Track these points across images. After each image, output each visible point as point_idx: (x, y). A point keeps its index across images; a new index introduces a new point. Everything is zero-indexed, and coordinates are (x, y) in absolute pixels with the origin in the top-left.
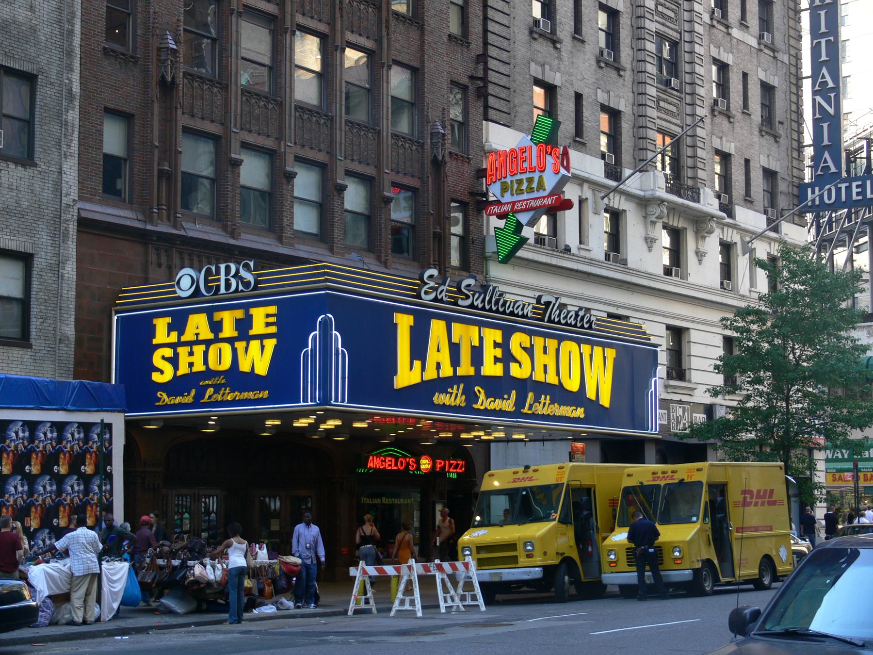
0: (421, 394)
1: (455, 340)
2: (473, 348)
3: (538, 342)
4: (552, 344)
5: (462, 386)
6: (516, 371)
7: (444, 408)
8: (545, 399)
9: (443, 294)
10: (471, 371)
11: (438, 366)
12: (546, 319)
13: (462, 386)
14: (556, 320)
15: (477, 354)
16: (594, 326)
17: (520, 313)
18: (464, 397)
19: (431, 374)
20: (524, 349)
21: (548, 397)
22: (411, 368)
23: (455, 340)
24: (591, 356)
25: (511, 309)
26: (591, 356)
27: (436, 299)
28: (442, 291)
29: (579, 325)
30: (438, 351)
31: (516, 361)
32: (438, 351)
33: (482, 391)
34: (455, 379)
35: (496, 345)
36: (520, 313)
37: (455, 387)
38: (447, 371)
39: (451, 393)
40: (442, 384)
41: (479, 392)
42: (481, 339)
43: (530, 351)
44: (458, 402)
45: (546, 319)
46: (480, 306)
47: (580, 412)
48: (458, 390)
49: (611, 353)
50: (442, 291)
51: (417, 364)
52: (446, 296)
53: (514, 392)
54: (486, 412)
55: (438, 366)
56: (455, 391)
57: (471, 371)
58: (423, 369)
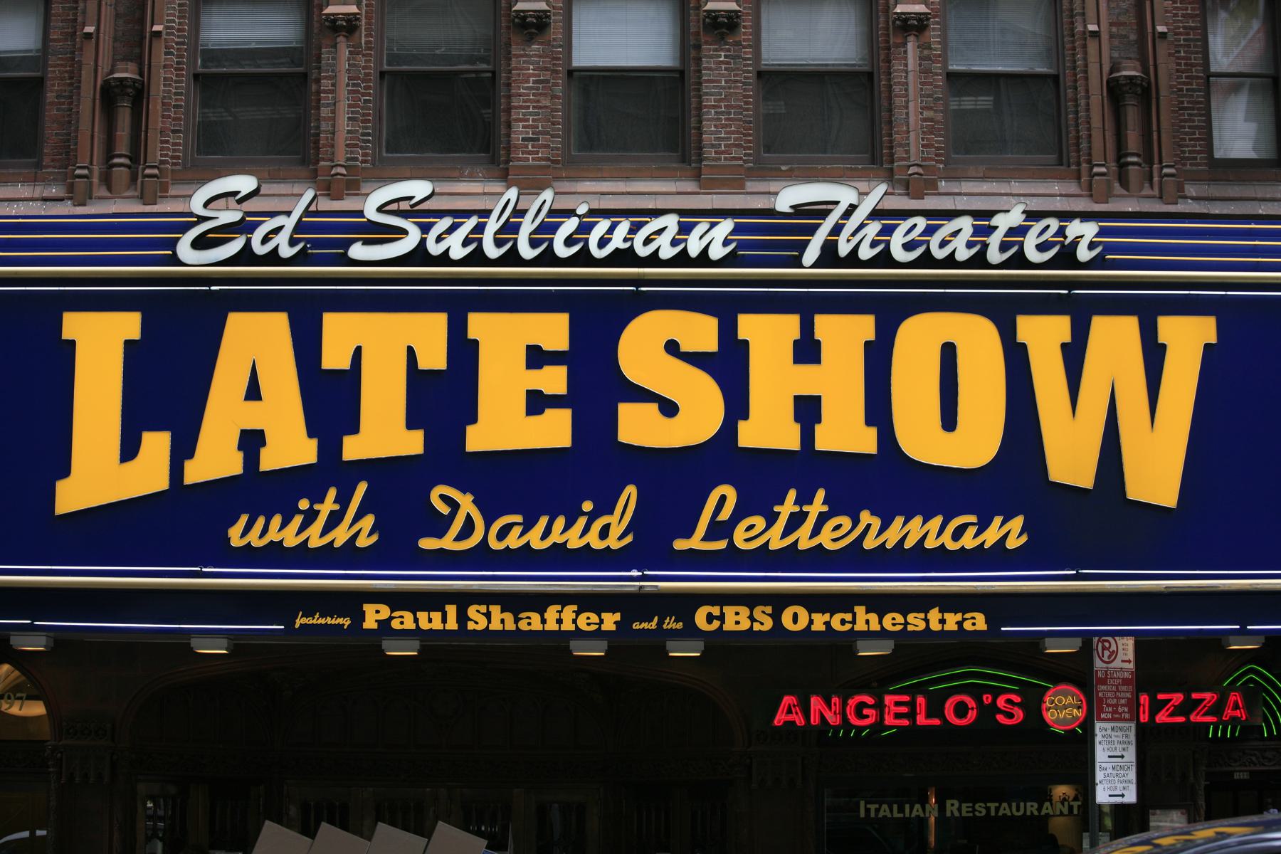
0: (181, 521)
1: (334, 357)
2: (417, 378)
3: (767, 335)
4: (845, 335)
5: (362, 488)
6: (637, 426)
7: (275, 555)
8: (805, 498)
9: (282, 240)
10: (413, 443)
11: (252, 441)
12: (812, 253)
13: (362, 488)
14: (866, 253)
15: (443, 397)
16: (1083, 254)
17: (667, 252)
18: (368, 521)
19: (215, 459)
20: (696, 359)
21: (820, 495)
22: (129, 450)
23: (334, 357)
24: (1074, 356)
25: (617, 242)
26: (1074, 356)
27: (246, 256)
28: (277, 231)
29: (994, 256)
30: (253, 392)
31: (642, 395)
32: (253, 392)
33: (467, 503)
34: (330, 472)
35: (537, 357)
36: (667, 252)
37: (332, 493)
38: (291, 447)
39: (311, 516)
40: (261, 490)
41: (444, 498)
42: (464, 352)
43: (729, 367)
44: (340, 536)
45: (812, 253)
46: (458, 252)
47: (1010, 531)
48: (344, 500)
49: (1188, 338)
50: (277, 231)
51: (156, 444)
52: (293, 242)
53: (631, 491)
54: (482, 558)
55: (252, 441)
56: (328, 506)
57: (413, 443)
58: (183, 449)
